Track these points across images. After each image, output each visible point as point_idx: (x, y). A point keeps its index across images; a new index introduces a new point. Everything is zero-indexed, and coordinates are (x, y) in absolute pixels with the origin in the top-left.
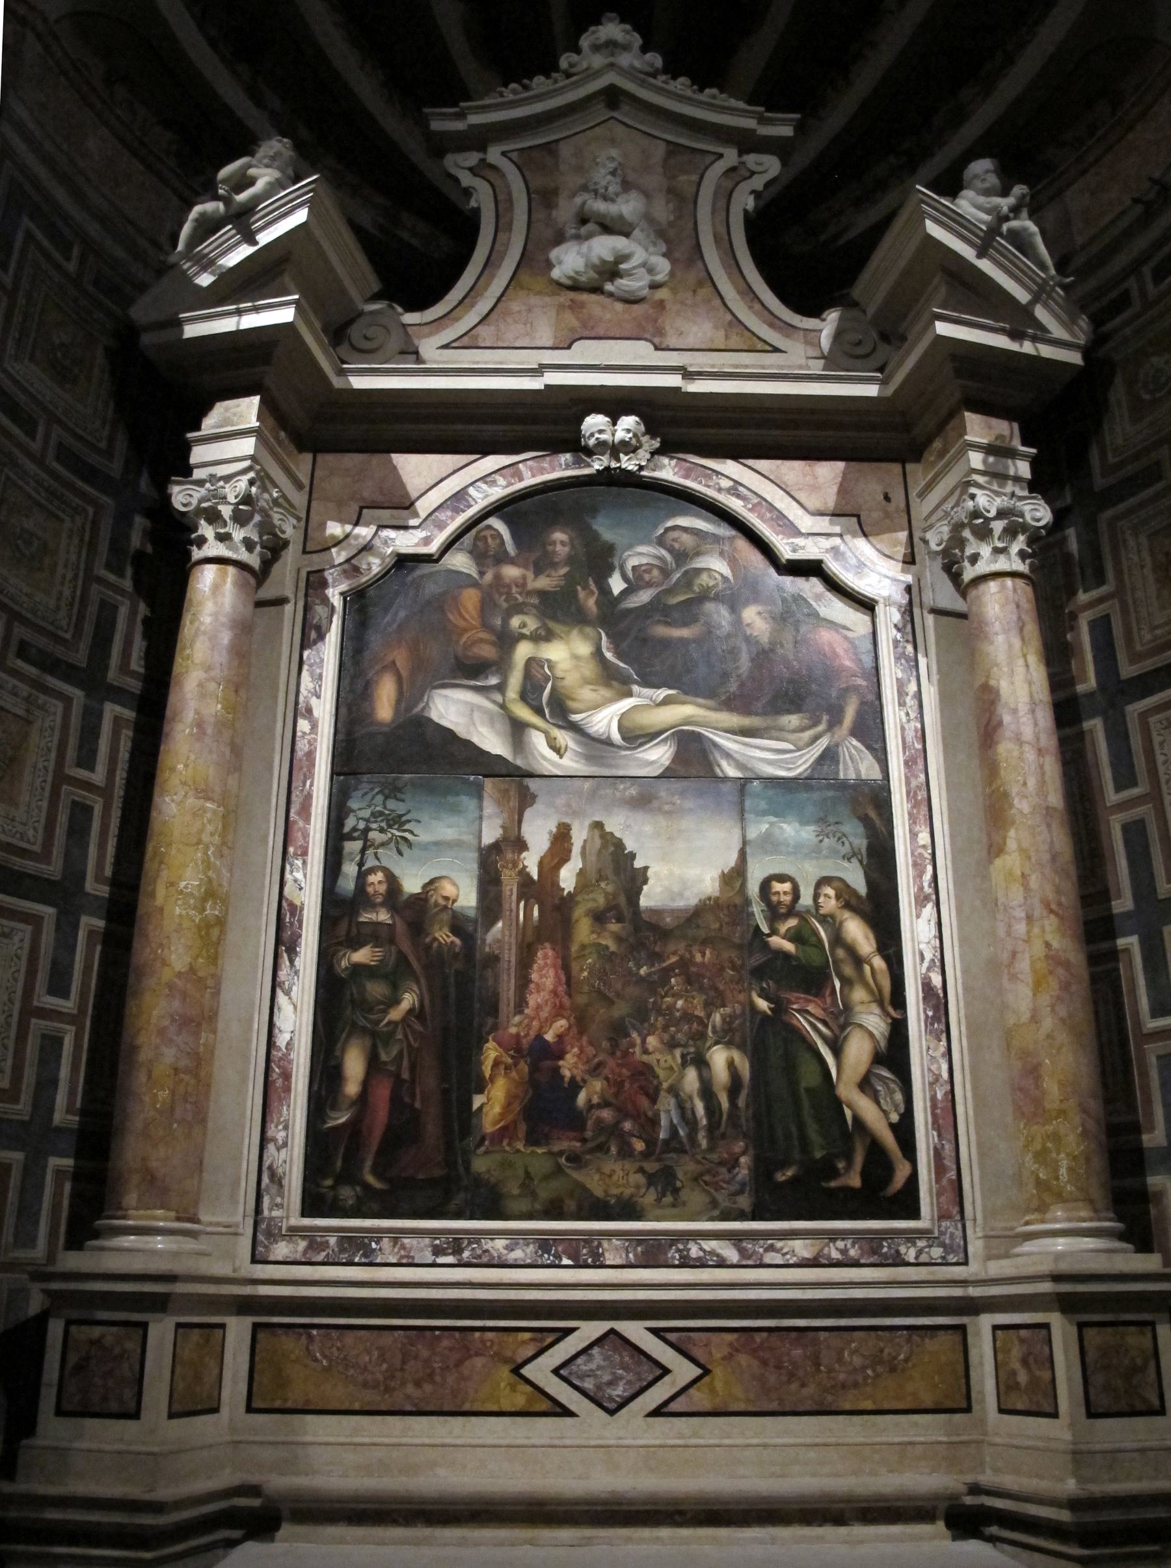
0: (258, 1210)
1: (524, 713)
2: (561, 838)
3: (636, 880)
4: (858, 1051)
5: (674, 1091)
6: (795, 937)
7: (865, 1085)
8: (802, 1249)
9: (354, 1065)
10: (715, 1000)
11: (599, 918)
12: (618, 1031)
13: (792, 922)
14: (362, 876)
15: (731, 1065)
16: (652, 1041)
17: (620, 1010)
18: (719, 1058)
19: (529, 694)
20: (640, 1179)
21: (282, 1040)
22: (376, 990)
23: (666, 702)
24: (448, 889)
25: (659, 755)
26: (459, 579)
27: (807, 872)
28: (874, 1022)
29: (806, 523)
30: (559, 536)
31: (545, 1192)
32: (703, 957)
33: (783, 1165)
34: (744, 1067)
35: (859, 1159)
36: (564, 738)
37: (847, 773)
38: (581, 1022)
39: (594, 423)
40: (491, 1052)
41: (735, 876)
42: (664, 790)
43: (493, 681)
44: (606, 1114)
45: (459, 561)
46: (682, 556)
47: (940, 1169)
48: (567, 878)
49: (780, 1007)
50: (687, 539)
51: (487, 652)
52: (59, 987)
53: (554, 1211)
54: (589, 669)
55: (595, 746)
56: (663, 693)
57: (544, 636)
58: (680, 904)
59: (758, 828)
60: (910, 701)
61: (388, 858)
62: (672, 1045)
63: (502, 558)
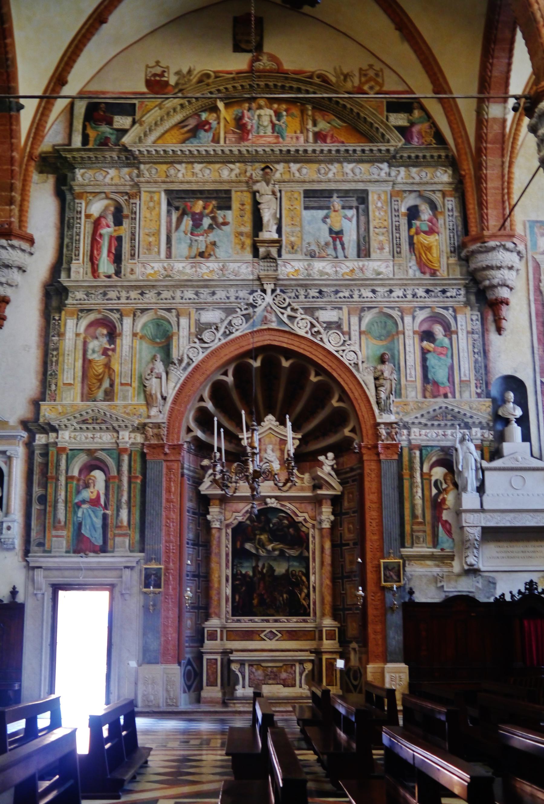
1: (258, 547)
3: (274, 571)
4: (303, 595)
8: (295, 620)
9: (237, 598)
18: (285, 596)
25: (277, 553)
27: (297, 570)
29: (300, 514)
39: (268, 500)
40: (255, 595)
41: (287, 571)
45: (248, 522)
46: (281, 520)
55: (268, 551)
57: (261, 534)
59: (291, 563)
61: (240, 569)
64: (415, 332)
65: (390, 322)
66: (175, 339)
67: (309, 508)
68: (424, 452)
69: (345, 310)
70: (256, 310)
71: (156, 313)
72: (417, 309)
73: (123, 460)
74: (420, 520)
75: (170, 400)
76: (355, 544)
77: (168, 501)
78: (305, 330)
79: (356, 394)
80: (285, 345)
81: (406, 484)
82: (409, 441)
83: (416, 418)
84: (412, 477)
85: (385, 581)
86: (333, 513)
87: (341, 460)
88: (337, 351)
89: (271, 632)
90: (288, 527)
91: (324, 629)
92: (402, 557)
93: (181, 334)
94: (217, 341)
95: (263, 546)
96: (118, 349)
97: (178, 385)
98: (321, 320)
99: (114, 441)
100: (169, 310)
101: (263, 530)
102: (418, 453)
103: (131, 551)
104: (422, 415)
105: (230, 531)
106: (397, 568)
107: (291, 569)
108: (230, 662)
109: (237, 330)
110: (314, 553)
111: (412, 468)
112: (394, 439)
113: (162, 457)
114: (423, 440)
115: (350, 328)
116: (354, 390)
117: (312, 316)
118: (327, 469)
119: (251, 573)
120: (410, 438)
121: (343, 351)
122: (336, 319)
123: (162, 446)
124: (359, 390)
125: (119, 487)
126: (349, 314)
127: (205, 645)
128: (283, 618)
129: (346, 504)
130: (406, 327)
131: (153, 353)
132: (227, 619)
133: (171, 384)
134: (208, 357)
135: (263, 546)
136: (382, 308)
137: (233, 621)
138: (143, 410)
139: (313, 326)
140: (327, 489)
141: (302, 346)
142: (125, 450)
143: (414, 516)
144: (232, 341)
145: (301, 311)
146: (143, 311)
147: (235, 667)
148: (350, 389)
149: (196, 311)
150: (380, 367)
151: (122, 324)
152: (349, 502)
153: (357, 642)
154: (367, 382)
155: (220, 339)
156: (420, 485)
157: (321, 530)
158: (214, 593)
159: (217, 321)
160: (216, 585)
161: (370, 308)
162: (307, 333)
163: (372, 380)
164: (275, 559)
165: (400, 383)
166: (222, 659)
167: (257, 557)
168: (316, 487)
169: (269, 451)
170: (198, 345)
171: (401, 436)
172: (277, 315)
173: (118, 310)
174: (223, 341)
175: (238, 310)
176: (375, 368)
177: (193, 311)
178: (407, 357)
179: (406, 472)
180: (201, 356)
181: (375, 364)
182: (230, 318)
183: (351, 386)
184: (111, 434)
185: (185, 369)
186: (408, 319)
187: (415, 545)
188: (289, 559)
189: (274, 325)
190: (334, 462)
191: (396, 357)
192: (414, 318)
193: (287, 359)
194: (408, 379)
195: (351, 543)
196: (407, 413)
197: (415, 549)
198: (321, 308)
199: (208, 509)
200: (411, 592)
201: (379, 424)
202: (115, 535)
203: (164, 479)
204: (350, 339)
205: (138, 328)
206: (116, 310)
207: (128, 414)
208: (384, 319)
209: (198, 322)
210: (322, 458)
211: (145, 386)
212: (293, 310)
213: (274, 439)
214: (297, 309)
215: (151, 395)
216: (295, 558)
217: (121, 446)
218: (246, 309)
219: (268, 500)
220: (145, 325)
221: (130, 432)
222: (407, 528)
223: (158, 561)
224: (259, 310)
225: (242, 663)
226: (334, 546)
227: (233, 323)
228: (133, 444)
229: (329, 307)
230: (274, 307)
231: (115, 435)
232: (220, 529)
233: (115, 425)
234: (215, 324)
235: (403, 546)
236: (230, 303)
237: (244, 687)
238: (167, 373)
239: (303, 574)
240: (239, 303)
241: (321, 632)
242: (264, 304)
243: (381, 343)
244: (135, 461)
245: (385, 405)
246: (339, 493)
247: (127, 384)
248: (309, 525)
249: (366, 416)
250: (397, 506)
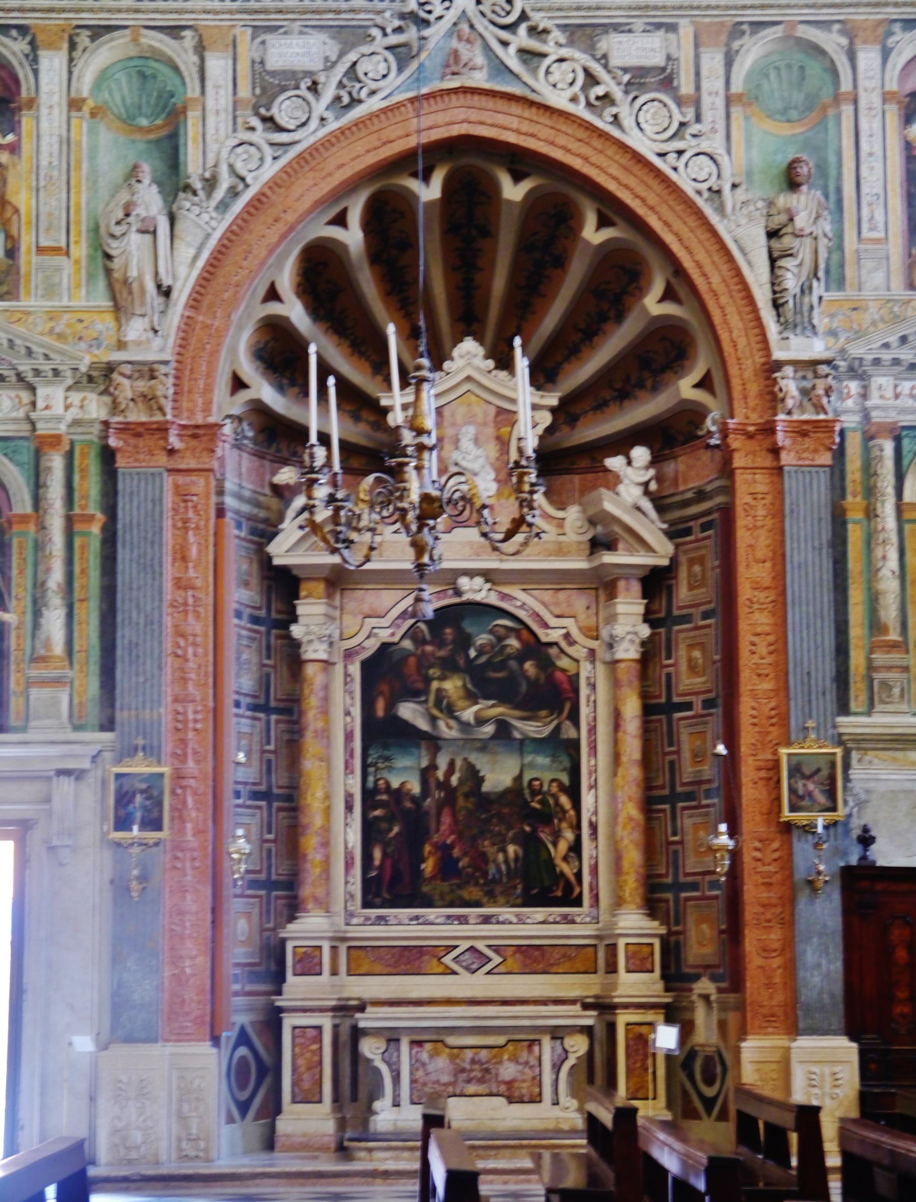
0: (346, 908)
1: (436, 712)
2: (452, 765)
4: (563, 846)
5: (495, 861)
6: (540, 802)
7: (565, 859)
9: (377, 854)
10: (509, 828)
11: (467, 796)
12: (474, 839)
13: (539, 797)
14: (376, 781)
15: (516, 852)
16: (486, 843)
17: (475, 831)
18: (511, 849)
19: (438, 703)
20: (481, 893)
21: (350, 845)
22: (384, 825)
23: (493, 706)
24: (408, 786)
25: (489, 729)
26: (407, 654)
27: (547, 776)
28: (569, 835)
29: (553, 622)
30: (448, 631)
31: (448, 898)
32: (506, 811)
33: (534, 888)
34: (520, 852)
35: (561, 885)
36: (452, 723)
37: (564, 736)
38: (460, 837)
40: (427, 848)
41: (518, 779)
42: (491, 745)
43: (423, 699)
44: (470, 870)
45: (407, 644)
46: (500, 639)
47: (591, 890)
48: (454, 780)
49: (534, 831)
50: (502, 631)
51: (419, 685)
52: (270, 832)
53: (451, 905)
54: (461, 693)
55: (465, 726)
56: (491, 702)
57: (442, 678)
58: (497, 790)
59: (528, 759)
60: (591, 704)
61: (386, 774)
62: (493, 844)
63: (424, 642)
64: (887, 97)
65: (815, 68)
66: (193, 116)
67: (580, 602)
68: (906, 443)
69: (686, 30)
70: (426, 33)
71: (135, 40)
72: (897, 27)
73: (49, 469)
74: (894, 636)
75: (181, 296)
76: (709, 704)
77: (181, 584)
78: (569, 93)
79: (715, 279)
80: (512, 138)
81: (855, 535)
82: (866, 414)
83: (886, 346)
84: (871, 514)
85: (793, 808)
86: (648, 618)
87: (670, 468)
88: (662, 155)
89: (472, 949)
90: (521, 657)
91: (621, 943)
92: (840, 741)
93: (210, 103)
94: (314, 124)
95: (450, 711)
96: (27, 147)
97: (205, 255)
98: (614, 62)
99: (21, 414)
100: (174, 31)
101: (449, 667)
102: (888, 447)
103: (77, 728)
104: (904, 339)
105: (355, 670)
106: (825, 772)
107: (527, 777)
108: (357, 1033)
109: (373, 93)
110: (592, 730)
111: (870, 492)
112: (820, 408)
113: (162, 459)
114: (903, 411)
115: (698, 88)
116: (708, 268)
117: (590, 49)
118: (630, 492)
119: (415, 788)
120: (869, 404)
121: (680, 153)
122: (658, 60)
123: (162, 429)
124: (725, 268)
125: (39, 547)
126: (697, 46)
127: (286, 988)
128: (507, 913)
129: (683, 593)
130: (862, 83)
131: (131, 161)
132: (350, 915)
133: (185, 252)
134: (289, 173)
135: (450, 711)
136: (792, 25)
137: (367, 921)
138: (105, 324)
139: (591, 79)
140: (631, 551)
141: (562, 140)
142: (55, 441)
143: (875, 625)
144: (358, 124)
145: (557, 35)
146: (98, 32)
147: (370, 1048)
148: (698, 265)
149: (253, 38)
150: (784, 200)
151: (36, 72)
152: (691, 587)
153: (714, 979)
154: (748, 245)
155: (323, 119)
156: (894, 538)
157: (613, 664)
158: (310, 843)
159: (316, 65)
160: (318, 821)
161: (758, 26)
162: (574, 100)
163: (762, 239)
164: (484, 747)
165: (840, 248)
166: (336, 1027)
167: (433, 742)
168: (597, 545)
169: (466, 443)
170: (260, 136)
171: (842, 399)
172: (487, 48)
173: (23, 30)
174: (333, 125)
175: (375, 32)
176: (771, 204)
177: (244, 36)
178: (864, 172)
179: (854, 502)
180: (270, 170)
181: (769, 191)
182: (352, 57)
183: (701, 256)
184: (13, 394)
185: (223, 206)
186: (868, 58)
187: (879, 707)
188: (523, 745)
189: (479, 79)
190: (652, 472)
191: (833, 172)
192: (886, 54)
193: (517, 177)
194: (865, 234)
195: (697, 701)
196: (859, 334)
197: (876, 719)
198: (617, 28)
199: (293, 608)
200: (866, 840)
201: (778, 365)
202: (29, 684)
203: (168, 523)
204: (698, 119)
205: (85, 85)
206: (19, 28)
207: (61, 337)
208: (798, 57)
209: (259, 65)
210: (615, 463)
211: (108, 257)
212: (533, 31)
213: (479, 410)
214: (546, 31)
215: (126, 282)
216: (540, 744)
217: (43, 429)
218: (399, 30)
219: (464, 582)
220: (103, 76)
221: (69, 389)
222: (857, 659)
223: (152, 751)
224: (436, 33)
225: (392, 1037)
226: (648, 710)
227: (360, 70)
228: (76, 423)
229: (639, 24)
230: (481, 25)
231: (25, 396)
232: (327, 664)
233: (25, 367)
234: (308, 73)
235: (843, 708)
236: (352, 11)
237: (396, 1104)
238: (172, 219)
239: (563, 788)
240: (380, 12)
241: (612, 949)
242: (451, 16)
243: (786, 130)
244: (84, 471)
245: (797, 310)
246: (665, 562)
247: (56, 250)
248: (578, 652)
249: (742, 342)
250: (827, 597)
